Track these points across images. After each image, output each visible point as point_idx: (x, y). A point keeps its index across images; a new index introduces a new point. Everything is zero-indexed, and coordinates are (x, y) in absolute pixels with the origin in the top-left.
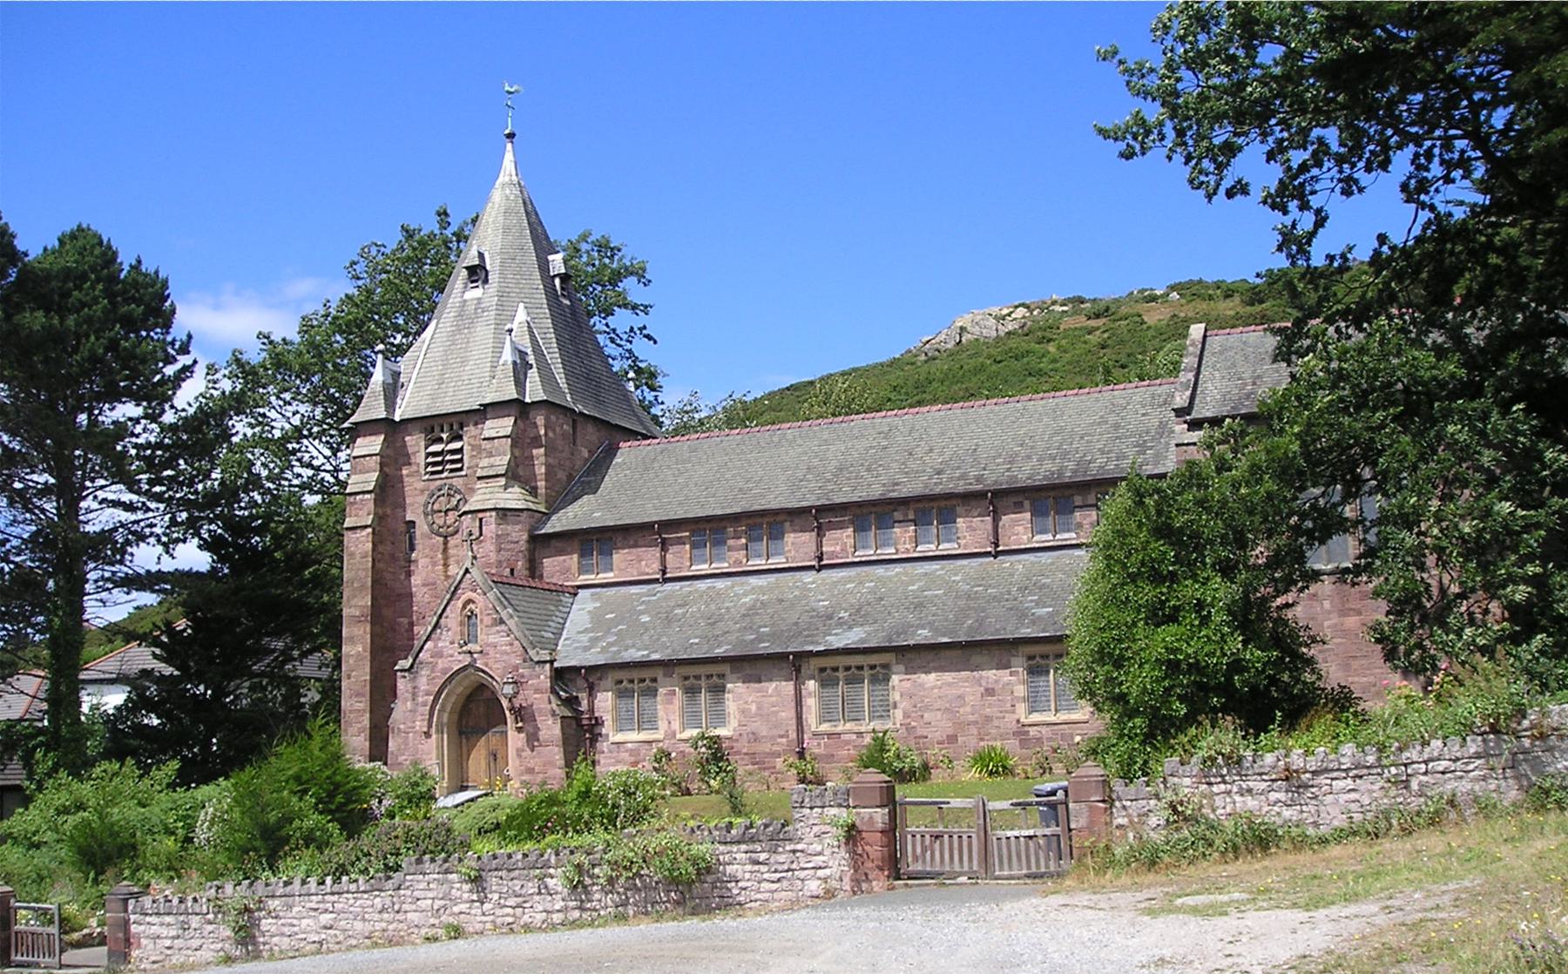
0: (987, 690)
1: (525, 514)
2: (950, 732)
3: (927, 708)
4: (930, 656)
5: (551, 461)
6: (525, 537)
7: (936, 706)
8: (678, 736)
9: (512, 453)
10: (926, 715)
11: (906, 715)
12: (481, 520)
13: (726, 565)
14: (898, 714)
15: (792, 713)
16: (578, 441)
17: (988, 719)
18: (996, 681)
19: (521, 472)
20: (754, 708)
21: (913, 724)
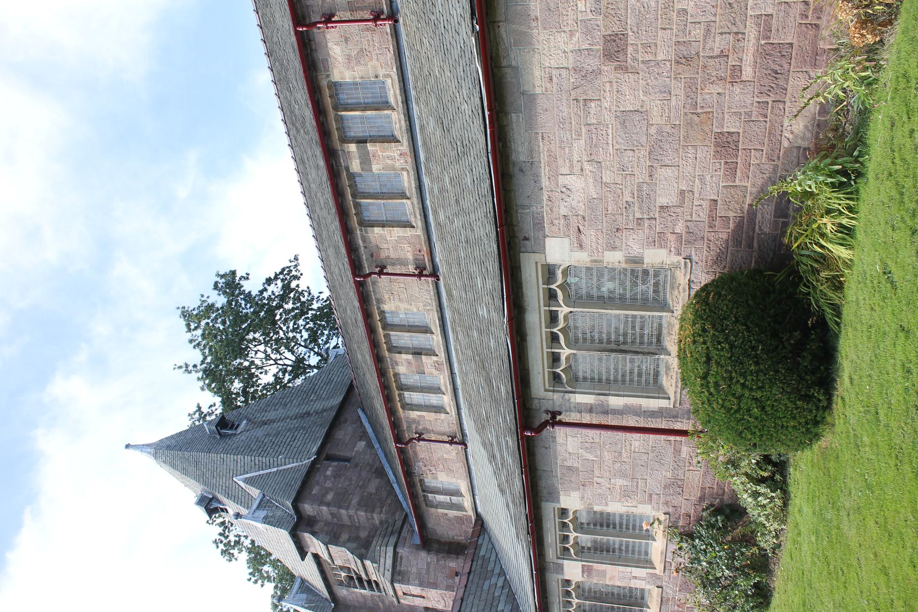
0: (609, 55)
1: (400, 550)
2: (706, 153)
3: (644, 196)
4: (523, 187)
5: (355, 501)
6: (423, 554)
7: (641, 175)
8: (659, 570)
9: (343, 545)
10: (663, 201)
11: (659, 241)
12: (404, 594)
13: (441, 377)
14: (654, 257)
15: (636, 436)
16: (348, 454)
17: (684, 60)
18: (588, 32)
19: (363, 534)
20: (620, 482)
21: (680, 228)
